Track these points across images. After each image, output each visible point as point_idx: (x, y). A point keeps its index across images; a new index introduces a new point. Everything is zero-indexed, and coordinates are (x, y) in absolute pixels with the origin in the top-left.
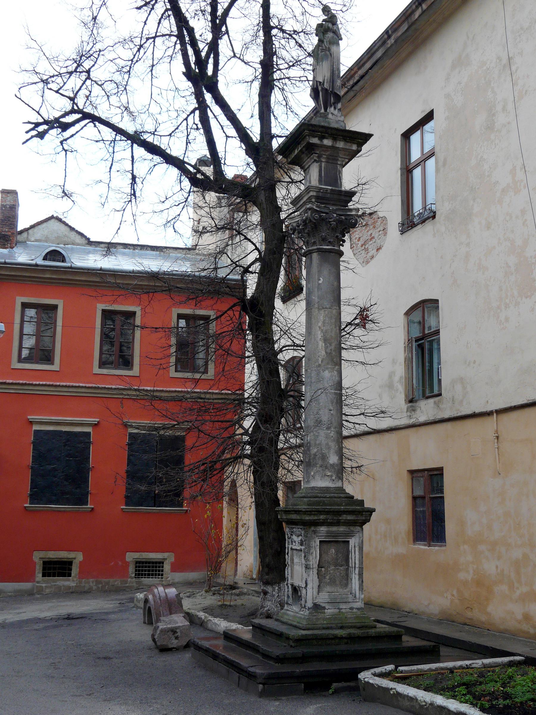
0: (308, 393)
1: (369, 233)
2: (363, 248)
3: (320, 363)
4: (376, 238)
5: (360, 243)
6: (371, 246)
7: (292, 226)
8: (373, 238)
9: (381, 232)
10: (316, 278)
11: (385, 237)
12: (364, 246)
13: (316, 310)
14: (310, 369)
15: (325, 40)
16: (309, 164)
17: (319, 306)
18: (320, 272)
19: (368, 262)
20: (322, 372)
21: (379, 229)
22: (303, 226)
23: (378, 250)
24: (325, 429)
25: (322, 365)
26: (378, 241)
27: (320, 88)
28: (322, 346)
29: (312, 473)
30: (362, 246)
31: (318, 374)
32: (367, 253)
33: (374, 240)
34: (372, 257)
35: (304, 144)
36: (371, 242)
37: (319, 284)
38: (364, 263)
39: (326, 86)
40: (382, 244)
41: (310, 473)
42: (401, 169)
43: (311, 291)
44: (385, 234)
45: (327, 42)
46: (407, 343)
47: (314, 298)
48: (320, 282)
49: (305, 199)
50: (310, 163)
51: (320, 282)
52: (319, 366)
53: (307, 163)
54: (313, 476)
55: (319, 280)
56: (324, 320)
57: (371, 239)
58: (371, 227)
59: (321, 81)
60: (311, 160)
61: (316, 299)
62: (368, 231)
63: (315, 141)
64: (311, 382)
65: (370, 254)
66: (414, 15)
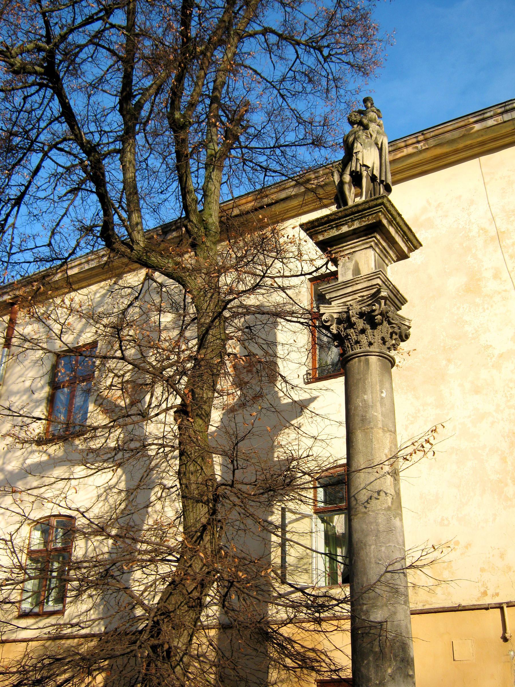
0: (373, 547)
3: (390, 504)
7: (332, 317)
10: (378, 389)
13: (380, 431)
14: (373, 511)
15: (370, 129)
16: (354, 250)
17: (383, 426)
18: (381, 382)
20: (393, 518)
24: (402, 602)
25: (393, 508)
27: (365, 173)
28: (391, 482)
29: (389, 671)
31: (389, 520)
35: (371, 220)
37: (382, 398)
39: (376, 173)
41: (386, 671)
43: (371, 404)
45: (373, 131)
47: (375, 414)
48: (384, 395)
49: (359, 287)
50: (357, 249)
51: (384, 395)
52: (389, 509)
53: (352, 248)
54: (391, 676)
55: (382, 392)
56: (391, 447)
59: (370, 165)
60: (363, 244)
61: (380, 417)
63: (385, 222)
64: (378, 531)
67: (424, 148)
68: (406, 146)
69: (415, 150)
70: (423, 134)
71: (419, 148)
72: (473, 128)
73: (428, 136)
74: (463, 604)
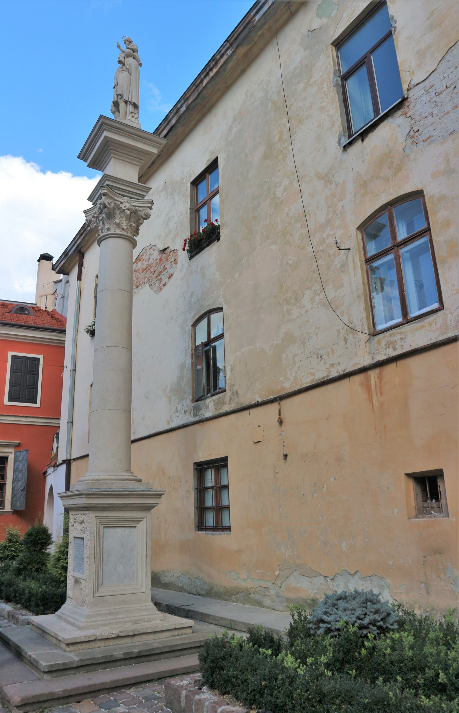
1: (163, 265)
2: (157, 279)
4: (168, 269)
5: (155, 276)
6: (164, 277)
8: (166, 268)
9: (172, 263)
11: (176, 266)
12: (158, 277)
19: (161, 289)
21: (171, 261)
22: (97, 214)
23: (169, 278)
26: (170, 271)
30: (156, 277)
32: (161, 282)
33: (166, 271)
34: (164, 285)
36: (164, 273)
38: (158, 291)
40: (173, 272)
42: (190, 209)
44: (176, 264)
46: (193, 350)
57: (164, 271)
58: (165, 260)
62: (161, 265)
65: (163, 283)
66: (203, 84)
67: (231, 52)
68: (222, 56)
69: (227, 56)
70: (228, 42)
71: (229, 54)
72: (255, 19)
73: (231, 41)
74: (260, 400)
